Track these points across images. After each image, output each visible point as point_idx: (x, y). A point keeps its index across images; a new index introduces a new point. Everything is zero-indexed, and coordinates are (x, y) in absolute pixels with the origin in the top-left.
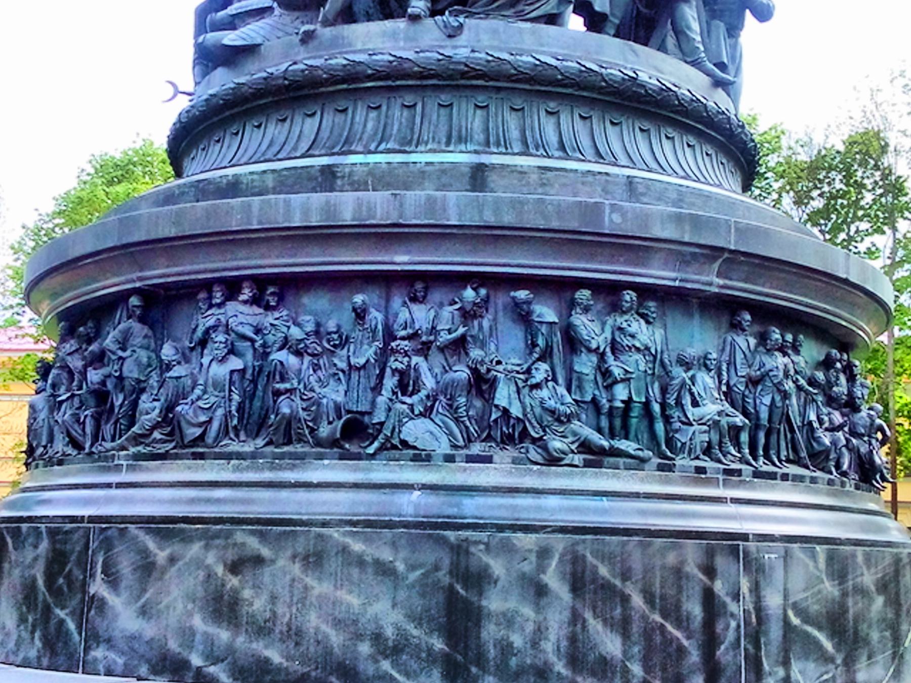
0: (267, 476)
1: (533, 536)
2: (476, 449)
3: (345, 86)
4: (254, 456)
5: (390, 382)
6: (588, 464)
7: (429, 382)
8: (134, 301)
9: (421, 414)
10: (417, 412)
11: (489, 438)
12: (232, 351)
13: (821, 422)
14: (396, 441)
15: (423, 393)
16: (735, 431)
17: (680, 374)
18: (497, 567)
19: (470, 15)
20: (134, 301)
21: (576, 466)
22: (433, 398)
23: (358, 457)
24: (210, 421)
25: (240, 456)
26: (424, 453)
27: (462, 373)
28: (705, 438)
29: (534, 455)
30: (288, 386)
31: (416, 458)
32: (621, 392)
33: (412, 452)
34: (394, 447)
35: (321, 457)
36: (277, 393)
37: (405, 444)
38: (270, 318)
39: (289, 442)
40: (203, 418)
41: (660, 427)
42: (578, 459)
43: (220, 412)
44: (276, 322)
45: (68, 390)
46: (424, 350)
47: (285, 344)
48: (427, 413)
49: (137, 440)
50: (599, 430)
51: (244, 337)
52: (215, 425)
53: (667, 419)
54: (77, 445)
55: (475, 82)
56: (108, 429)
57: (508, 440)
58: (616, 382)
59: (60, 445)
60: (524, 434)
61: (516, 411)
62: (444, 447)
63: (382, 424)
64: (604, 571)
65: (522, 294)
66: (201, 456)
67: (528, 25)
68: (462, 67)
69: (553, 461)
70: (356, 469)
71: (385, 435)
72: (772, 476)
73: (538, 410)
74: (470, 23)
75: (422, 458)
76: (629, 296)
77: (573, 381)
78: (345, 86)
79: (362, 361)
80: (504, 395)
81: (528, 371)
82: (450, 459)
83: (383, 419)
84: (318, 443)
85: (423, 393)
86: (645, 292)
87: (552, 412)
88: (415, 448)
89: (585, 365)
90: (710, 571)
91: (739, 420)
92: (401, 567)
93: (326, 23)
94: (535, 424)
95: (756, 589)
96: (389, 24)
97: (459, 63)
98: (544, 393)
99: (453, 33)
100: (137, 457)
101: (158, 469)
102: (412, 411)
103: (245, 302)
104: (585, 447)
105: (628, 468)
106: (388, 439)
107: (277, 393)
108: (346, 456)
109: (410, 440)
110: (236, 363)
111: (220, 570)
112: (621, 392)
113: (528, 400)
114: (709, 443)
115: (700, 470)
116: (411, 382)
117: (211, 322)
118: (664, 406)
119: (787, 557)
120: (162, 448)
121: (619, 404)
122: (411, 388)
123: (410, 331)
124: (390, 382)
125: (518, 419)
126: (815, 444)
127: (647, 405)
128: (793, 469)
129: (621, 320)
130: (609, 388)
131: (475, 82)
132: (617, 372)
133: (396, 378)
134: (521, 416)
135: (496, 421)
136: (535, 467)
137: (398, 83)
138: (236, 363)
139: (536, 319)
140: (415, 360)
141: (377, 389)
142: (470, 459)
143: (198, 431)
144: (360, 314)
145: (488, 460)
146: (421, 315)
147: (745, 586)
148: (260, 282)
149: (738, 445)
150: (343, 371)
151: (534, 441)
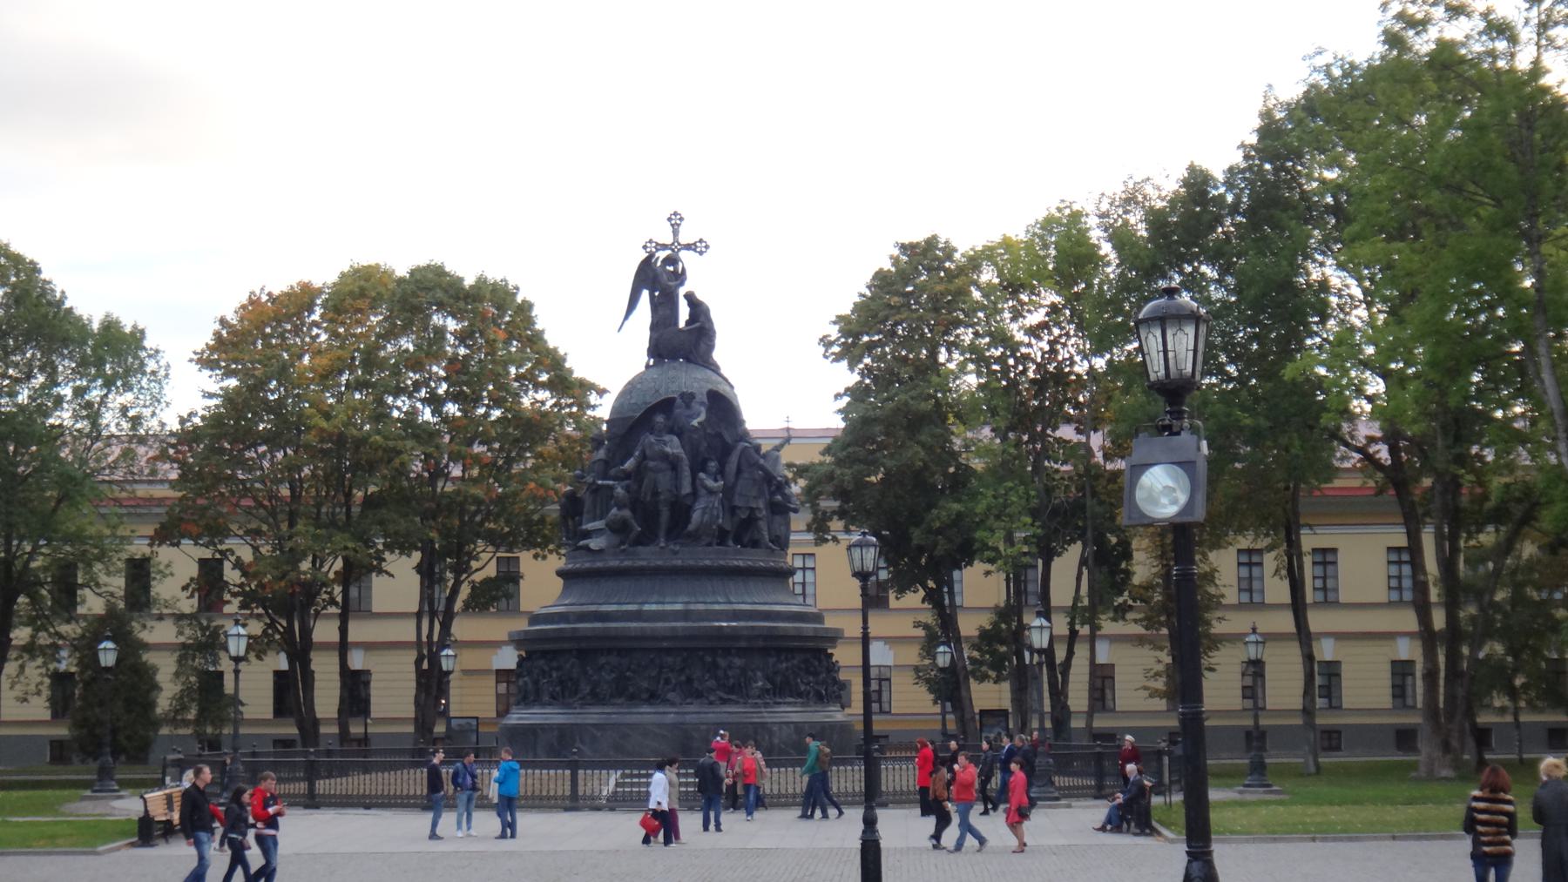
2: (689, 700)
4: (622, 704)
5: (662, 682)
7: (674, 681)
12: (612, 671)
13: (802, 682)
16: (767, 691)
17: (750, 673)
25: (618, 704)
27: (683, 678)
29: (706, 701)
32: (732, 681)
37: (668, 700)
41: (744, 690)
45: (544, 678)
46: (672, 671)
47: (629, 669)
48: (674, 690)
49: (581, 699)
54: (553, 697)
59: (546, 698)
62: (678, 700)
65: (701, 653)
69: (711, 703)
72: (780, 703)
75: (673, 704)
80: (696, 684)
82: (681, 704)
86: (739, 649)
89: (720, 673)
91: (769, 686)
95: (770, 738)
104: (721, 699)
108: (651, 704)
110: (613, 675)
117: (604, 661)
119: (780, 729)
124: (662, 682)
127: (740, 685)
128: (791, 700)
138: (613, 675)
140: (670, 675)
141: (659, 682)
145: (692, 704)
146: (670, 660)
147: (767, 738)
149: (768, 694)
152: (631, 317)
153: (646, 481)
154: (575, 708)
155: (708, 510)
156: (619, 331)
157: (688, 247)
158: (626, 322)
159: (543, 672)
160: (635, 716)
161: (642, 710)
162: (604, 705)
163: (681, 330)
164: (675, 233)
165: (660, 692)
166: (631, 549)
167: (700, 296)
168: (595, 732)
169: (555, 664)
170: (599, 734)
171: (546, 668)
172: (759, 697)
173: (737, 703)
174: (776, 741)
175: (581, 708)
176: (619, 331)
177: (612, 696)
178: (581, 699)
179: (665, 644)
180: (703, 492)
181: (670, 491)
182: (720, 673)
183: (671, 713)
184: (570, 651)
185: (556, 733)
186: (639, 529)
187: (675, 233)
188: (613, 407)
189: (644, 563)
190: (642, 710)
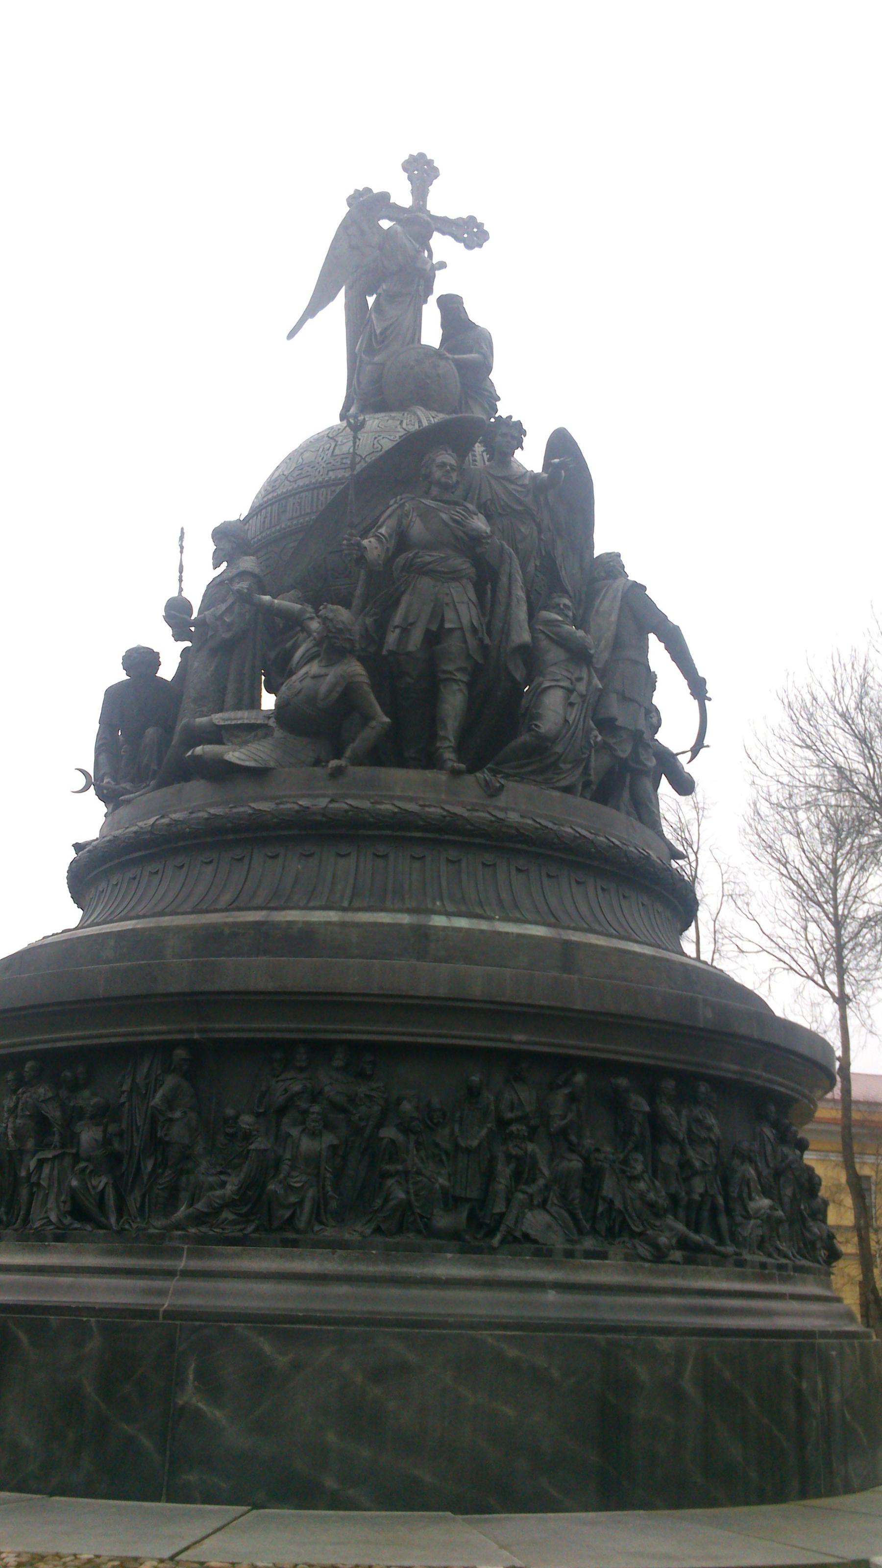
0: (382, 1269)
1: (672, 1339)
2: (589, 1243)
3: (389, 832)
6: (688, 1261)
8: (180, 1053)
9: (538, 1206)
10: (535, 1202)
11: (594, 1231)
14: (518, 1234)
15: (541, 1182)
18: (643, 1373)
19: (507, 776)
20: (180, 1053)
21: (678, 1263)
22: (547, 1187)
23: (478, 1251)
24: (301, 1203)
26: (544, 1247)
28: (760, 1232)
29: (643, 1250)
30: (400, 1167)
31: (538, 1253)
32: (699, 1186)
33: (533, 1246)
34: (516, 1240)
35: (440, 1250)
36: (386, 1175)
37: (526, 1237)
38: (362, 1090)
39: (400, 1229)
40: (293, 1199)
41: (723, 1220)
42: (677, 1255)
43: (311, 1193)
44: (373, 1093)
45: (42, 1145)
48: (543, 1205)
49: (199, 1219)
50: (688, 1226)
51: (342, 1110)
52: (307, 1207)
53: (729, 1211)
55: (519, 846)
56: (133, 1200)
57: (611, 1234)
58: (695, 1173)
60: (624, 1227)
61: (618, 1204)
62: (558, 1241)
63: (502, 1215)
64: (727, 1374)
65: (623, 1082)
66: (294, 1244)
67: (557, 794)
68: (513, 831)
69: (659, 1256)
70: (480, 1265)
71: (508, 1226)
73: (638, 1204)
74: (510, 785)
76: (703, 1088)
77: (656, 1169)
78: (389, 832)
79: (475, 1143)
80: (609, 1187)
81: (625, 1162)
82: (569, 1254)
83: (504, 1210)
84: (431, 1232)
85: (541, 1182)
87: (651, 1205)
88: (535, 1242)
89: (668, 1156)
90: (799, 1371)
92: (556, 1374)
93: (357, 761)
94: (635, 1218)
96: (429, 774)
97: (510, 827)
98: (642, 1186)
99: (493, 792)
100: (202, 1240)
101: (237, 1255)
102: (532, 1201)
103: (338, 1069)
104: (683, 1244)
105: (717, 1264)
106: (509, 1232)
107: (386, 1175)
109: (532, 1232)
110: (329, 1139)
111: (359, 1378)
112: (699, 1186)
113: (629, 1193)
114: (762, 1238)
115: (763, 1266)
116: (527, 1170)
118: (727, 1198)
120: (231, 1231)
121: (696, 1197)
122: (525, 1176)
123: (520, 1113)
125: (620, 1211)
126: (808, 1235)
129: (697, 1111)
130: (687, 1180)
131: (519, 846)
132: (697, 1164)
133: (513, 1166)
134: (622, 1208)
135: (602, 1214)
136: (647, 1265)
137: (446, 837)
138: (329, 1139)
139: (632, 1108)
141: (490, 1176)
142: (590, 1254)
143: (287, 1214)
144: (473, 1093)
145: (603, 1256)
146: (526, 1095)
148: (355, 1048)
150: (447, 1154)
151: (633, 1235)
152: (321, 314)
153: (405, 600)
154: (176, 1253)
155: (574, 698)
156: (292, 335)
157: (448, 226)
158: (310, 322)
159: (42, 1124)
160: (415, 1292)
161: (441, 1270)
162: (287, 1243)
163: (436, 353)
164: (420, 191)
165: (499, 1208)
166: (362, 771)
167: (475, 313)
168: (267, 1348)
169: (87, 1099)
170: (282, 1361)
171: (54, 1113)
172: (761, 1245)
173: (722, 1259)
174: (836, 1397)
175: (192, 1254)
176: (292, 335)
177: (317, 1215)
178: (199, 1219)
179: (520, 1038)
180: (554, 654)
181: (474, 630)
182: (668, 1156)
183: (540, 1286)
184: (165, 1048)
185: (94, 1344)
186: (387, 720)
187: (420, 191)
188: (272, 484)
189: (411, 807)
190: (441, 1270)
